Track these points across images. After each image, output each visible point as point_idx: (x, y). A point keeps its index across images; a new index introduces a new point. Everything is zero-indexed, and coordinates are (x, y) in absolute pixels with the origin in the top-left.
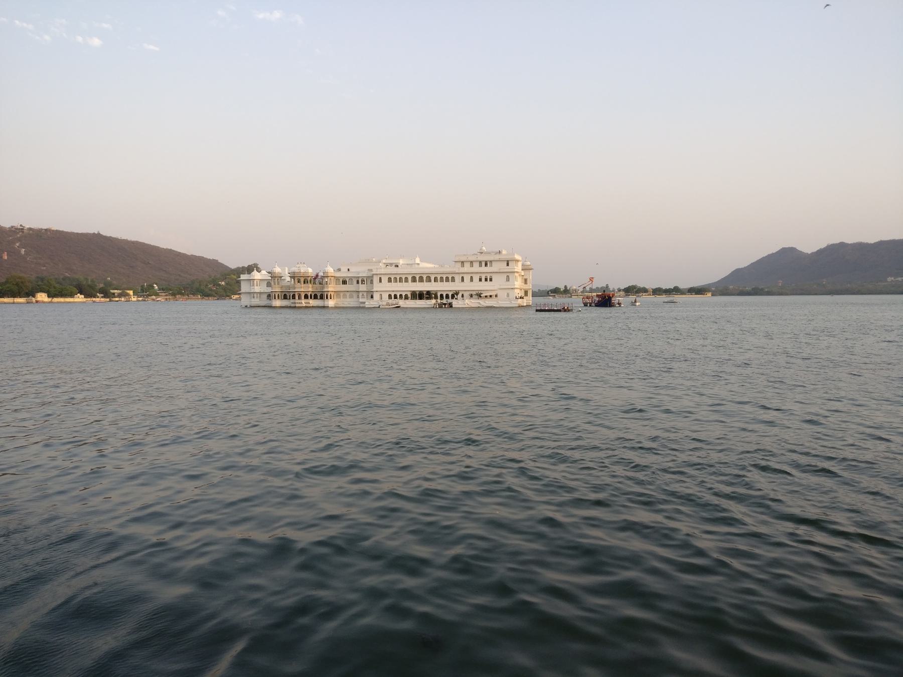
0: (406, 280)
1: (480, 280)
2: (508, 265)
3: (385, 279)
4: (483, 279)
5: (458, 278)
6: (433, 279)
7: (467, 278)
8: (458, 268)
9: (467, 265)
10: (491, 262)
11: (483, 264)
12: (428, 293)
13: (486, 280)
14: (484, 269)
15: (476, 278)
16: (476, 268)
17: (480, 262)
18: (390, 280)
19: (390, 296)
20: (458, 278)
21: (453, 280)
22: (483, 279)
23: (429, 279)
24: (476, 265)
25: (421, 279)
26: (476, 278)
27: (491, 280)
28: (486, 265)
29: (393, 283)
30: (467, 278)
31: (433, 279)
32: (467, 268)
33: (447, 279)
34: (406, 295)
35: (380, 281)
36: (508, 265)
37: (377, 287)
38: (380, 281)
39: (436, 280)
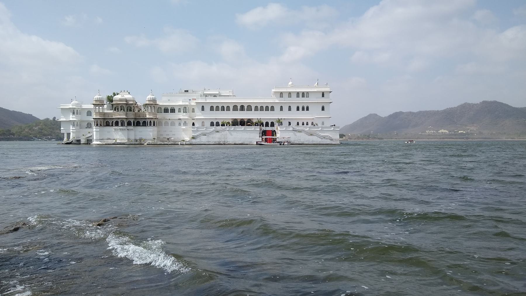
0: (228, 108)
1: (298, 109)
2: (323, 96)
4: (301, 109)
5: (277, 108)
6: (253, 108)
7: (286, 108)
9: (286, 96)
10: (308, 93)
11: (301, 95)
15: (294, 108)
16: (294, 100)
18: (212, 109)
19: (212, 124)
20: (277, 108)
21: (273, 109)
22: (301, 109)
23: (249, 108)
24: (294, 96)
25: (242, 108)
26: (294, 108)
27: (308, 109)
28: (303, 96)
30: (286, 108)
31: (253, 108)
32: (286, 100)
34: (229, 123)
36: (323, 96)
39: (256, 109)
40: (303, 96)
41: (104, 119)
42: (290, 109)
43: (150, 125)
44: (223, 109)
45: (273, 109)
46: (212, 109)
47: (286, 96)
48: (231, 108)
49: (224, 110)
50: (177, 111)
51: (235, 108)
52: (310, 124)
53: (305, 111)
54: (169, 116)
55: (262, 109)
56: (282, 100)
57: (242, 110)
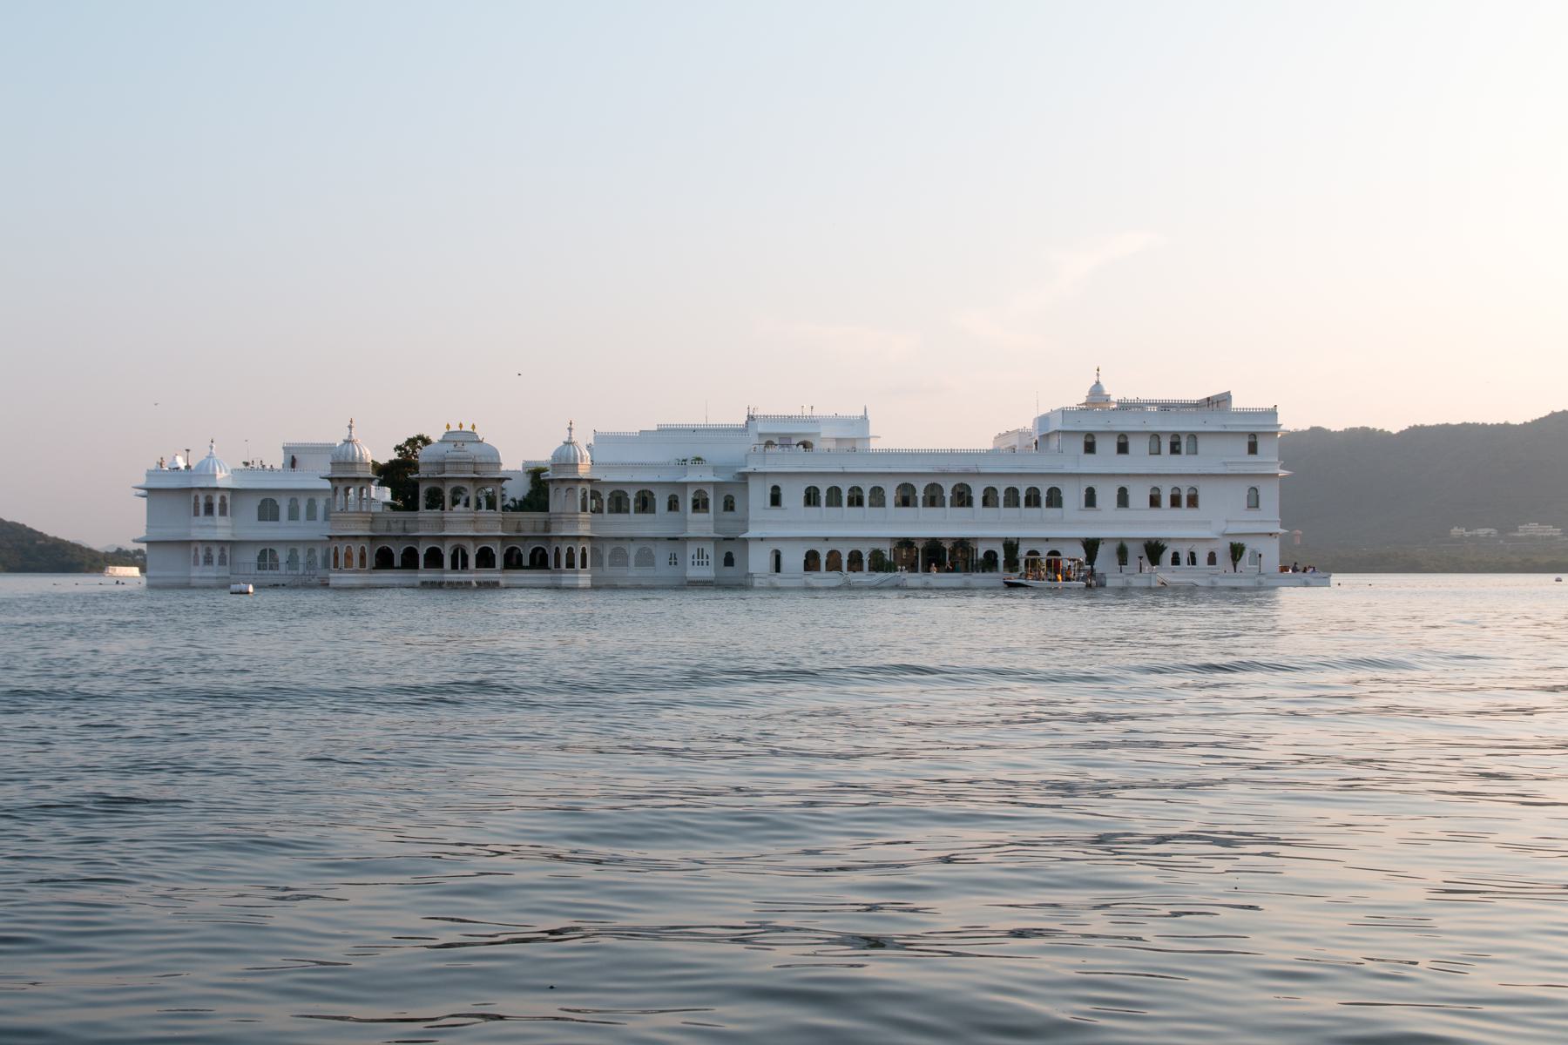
0: (878, 497)
1: (1155, 502)
2: (1253, 449)
3: (793, 495)
4: (1166, 500)
6: (978, 496)
7: (1107, 495)
8: (1073, 460)
9: (1106, 446)
10: (1193, 436)
11: (1166, 446)
12: (963, 544)
13: (1175, 501)
14: (1167, 463)
15: (1139, 495)
16: (1139, 460)
17: (1156, 436)
18: (811, 498)
20: (1073, 496)
21: (1055, 499)
22: (1166, 500)
23: (962, 498)
25: (933, 498)
26: (1139, 495)
27: (1193, 501)
28: (1175, 449)
29: (823, 511)
30: (1107, 495)
31: (978, 496)
32: (1106, 459)
33: (1033, 500)
35: (776, 500)
36: (1253, 449)
37: (761, 522)
38: (776, 500)
39: (989, 499)
40: (1175, 449)
41: (372, 538)
42: (1123, 499)
43: (570, 565)
44: (856, 500)
45: (1055, 499)
46: (811, 498)
47: (1106, 446)
48: (891, 495)
49: (1038, 504)
50: (661, 502)
51: (906, 499)
52: (1202, 558)
53: (1184, 512)
54: (632, 524)
55: (1012, 498)
56: (1089, 464)
57: (962, 505)
